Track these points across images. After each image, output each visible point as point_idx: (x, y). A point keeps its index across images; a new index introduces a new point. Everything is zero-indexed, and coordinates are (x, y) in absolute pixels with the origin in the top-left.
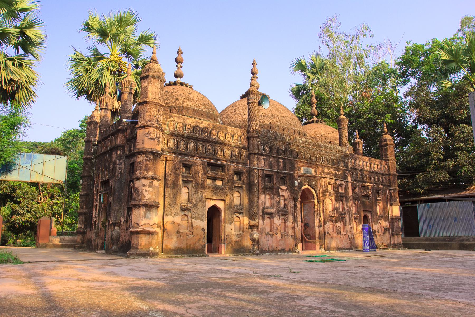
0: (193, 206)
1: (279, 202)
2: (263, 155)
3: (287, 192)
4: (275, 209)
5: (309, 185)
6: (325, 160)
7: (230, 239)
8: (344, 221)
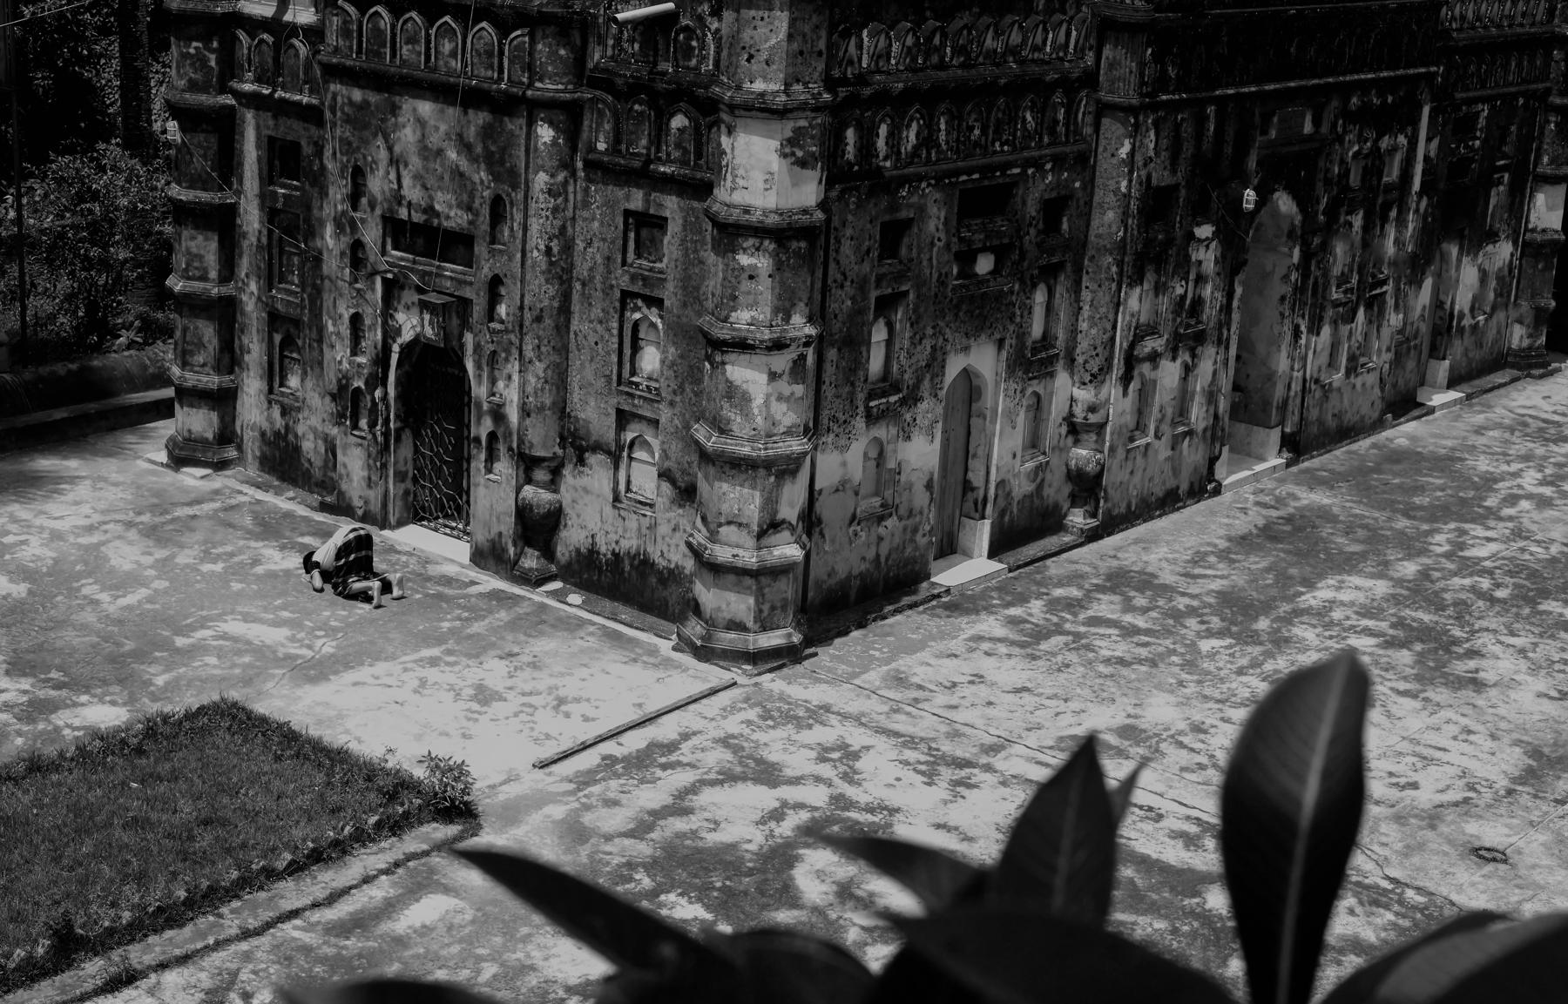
2: (1155, 107)
3: (1214, 243)
5: (1284, 189)
7: (1009, 494)
8: (1376, 309)
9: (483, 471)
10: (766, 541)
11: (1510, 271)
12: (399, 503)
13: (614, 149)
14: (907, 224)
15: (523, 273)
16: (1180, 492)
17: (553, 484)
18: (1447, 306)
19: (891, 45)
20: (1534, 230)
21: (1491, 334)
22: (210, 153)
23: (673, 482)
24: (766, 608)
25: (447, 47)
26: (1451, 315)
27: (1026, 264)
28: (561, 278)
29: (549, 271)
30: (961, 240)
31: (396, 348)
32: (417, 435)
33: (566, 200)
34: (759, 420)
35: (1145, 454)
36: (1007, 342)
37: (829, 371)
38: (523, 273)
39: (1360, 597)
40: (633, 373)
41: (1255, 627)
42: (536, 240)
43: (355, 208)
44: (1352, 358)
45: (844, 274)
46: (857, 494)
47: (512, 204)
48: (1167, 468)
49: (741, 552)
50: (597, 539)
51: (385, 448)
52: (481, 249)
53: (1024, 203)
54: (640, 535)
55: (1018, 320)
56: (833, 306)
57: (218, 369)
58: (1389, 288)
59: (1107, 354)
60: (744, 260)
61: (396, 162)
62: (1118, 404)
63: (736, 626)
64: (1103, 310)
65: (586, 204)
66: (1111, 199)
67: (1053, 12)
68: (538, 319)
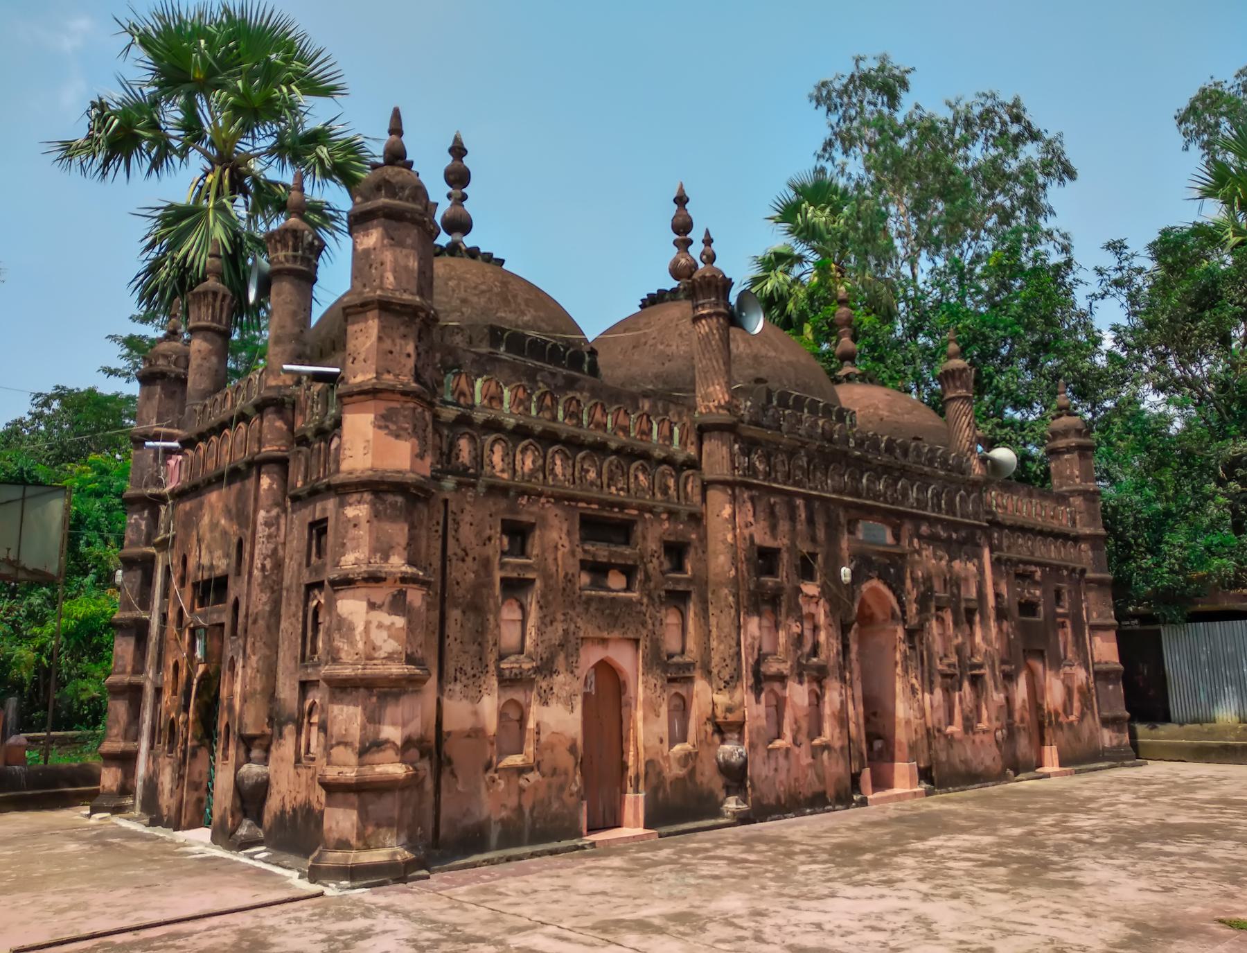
1: (800, 638)
2: (749, 486)
3: (822, 602)
4: (789, 663)
5: (879, 577)
6: (921, 496)
7: (660, 773)
10: (368, 758)
12: (191, 808)
13: (305, 483)
14: (532, 526)
16: (828, 796)
17: (265, 761)
20: (1099, 663)
21: (1085, 733)
26: (1049, 713)
27: (652, 585)
29: (263, 582)
30: (585, 551)
31: (195, 681)
33: (278, 529)
34: (360, 645)
37: (452, 629)
39: (968, 844)
40: (314, 651)
41: (860, 858)
42: (258, 563)
45: (464, 550)
48: (811, 773)
49: (345, 769)
51: (183, 762)
52: (230, 583)
53: (644, 538)
54: (308, 786)
55: (650, 627)
56: (454, 573)
57: (125, 738)
59: (735, 664)
60: (350, 512)
62: (755, 711)
63: (343, 845)
64: (726, 630)
65: (291, 529)
66: (721, 547)
67: (657, 415)
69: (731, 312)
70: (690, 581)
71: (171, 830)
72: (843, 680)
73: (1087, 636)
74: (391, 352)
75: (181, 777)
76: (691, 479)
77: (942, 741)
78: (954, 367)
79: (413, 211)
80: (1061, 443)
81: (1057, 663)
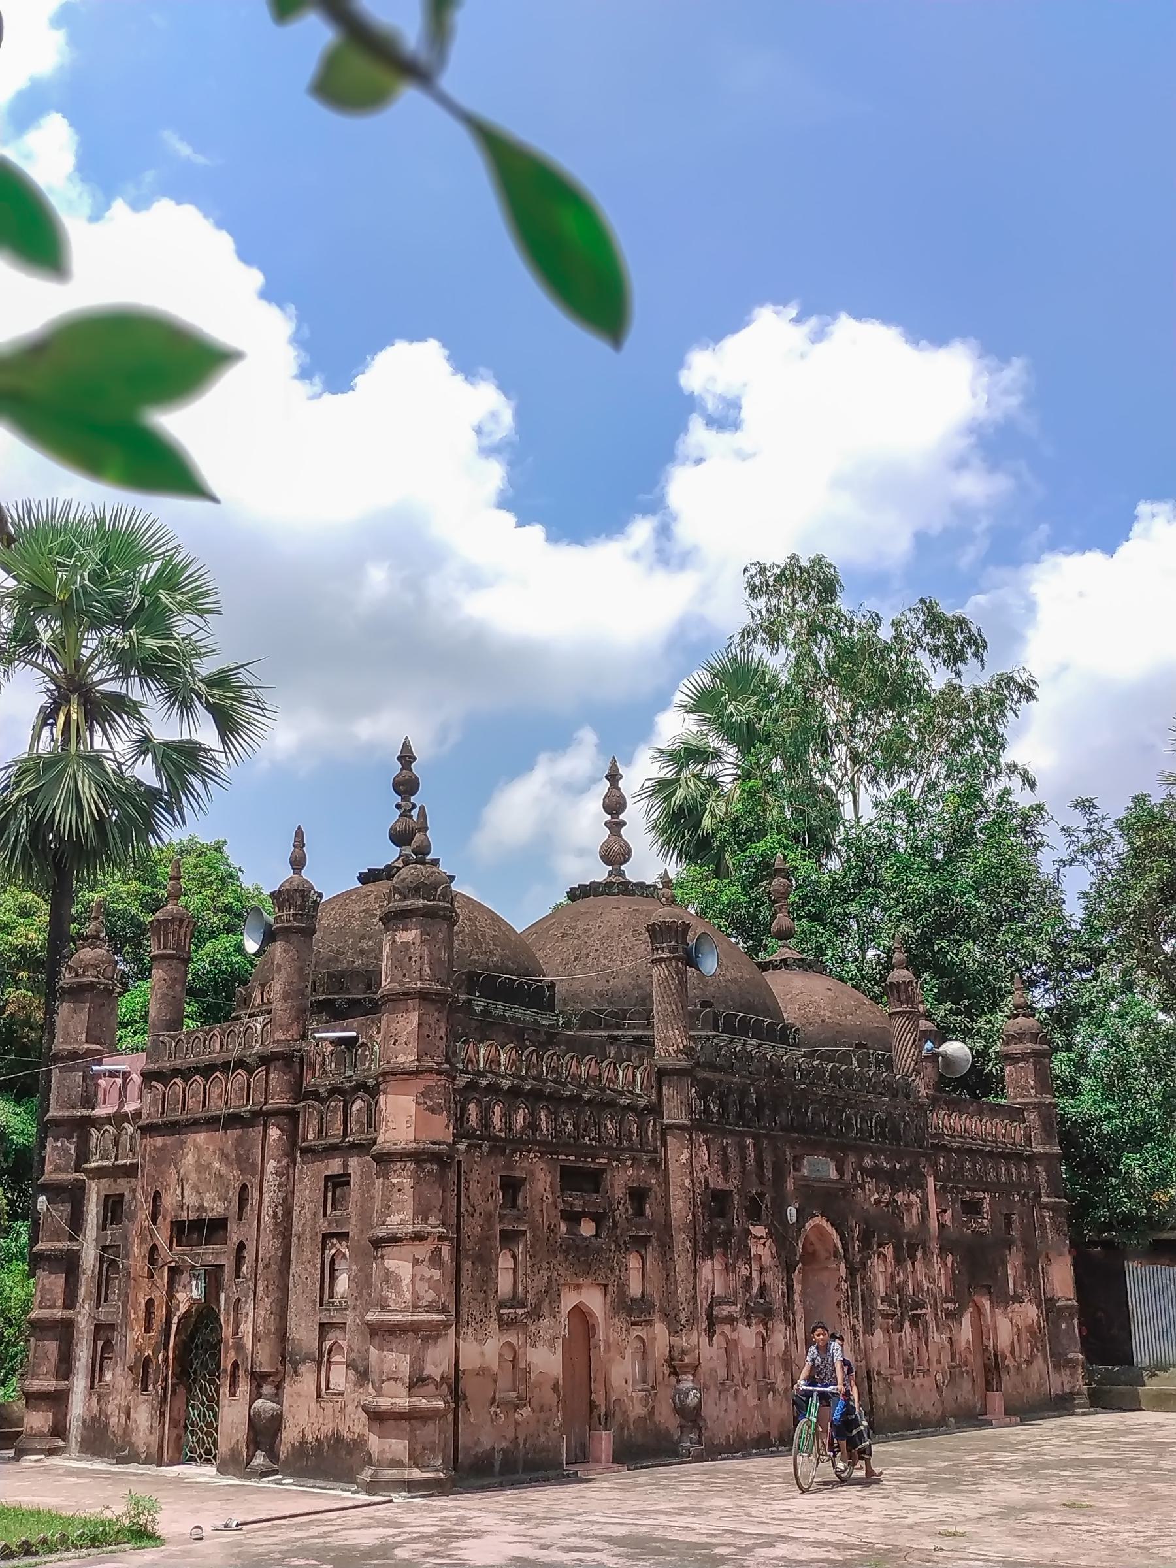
0: (528, 1315)
1: (749, 1278)
2: (704, 1131)
3: (767, 1244)
7: (625, 1412)
9: (228, 1393)
10: (415, 1391)
11: (1039, 1328)
12: (172, 1445)
14: (523, 1180)
15: (258, 1235)
17: (277, 1397)
18: (991, 1348)
19: (500, 1055)
20: (1051, 1299)
21: (1035, 1378)
22: (65, 1214)
23: (356, 1369)
24: (419, 1447)
25: (217, 1091)
26: (996, 1355)
27: (619, 1231)
28: (284, 1234)
31: (175, 1320)
32: (189, 1390)
33: (288, 1178)
34: (408, 1295)
35: (735, 1398)
36: (610, 1288)
38: (258, 1235)
42: (267, 1208)
43: (154, 1221)
44: (907, 1361)
46: (495, 1381)
47: (252, 1187)
49: (397, 1401)
50: (305, 1433)
51: (163, 1400)
52: (232, 1226)
53: (612, 1185)
54: (335, 1418)
55: (617, 1273)
56: (465, 1229)
58: (927, 1310)
61: (181, 1181)
65: (301, 1179)
68: (267, 1266)
69: (688, 952)
70: (651, 1225)
71: (153, 1467)
72: (787, 1321)
73: (1040, 1268)
74: (428, 1036)
75: (162, 1414)
76: (652, 1123)
77: (882, 1385)
78: (900, 980)
79: (446, 909)
80: (1015, 1048)
81: (1003, 1299)
